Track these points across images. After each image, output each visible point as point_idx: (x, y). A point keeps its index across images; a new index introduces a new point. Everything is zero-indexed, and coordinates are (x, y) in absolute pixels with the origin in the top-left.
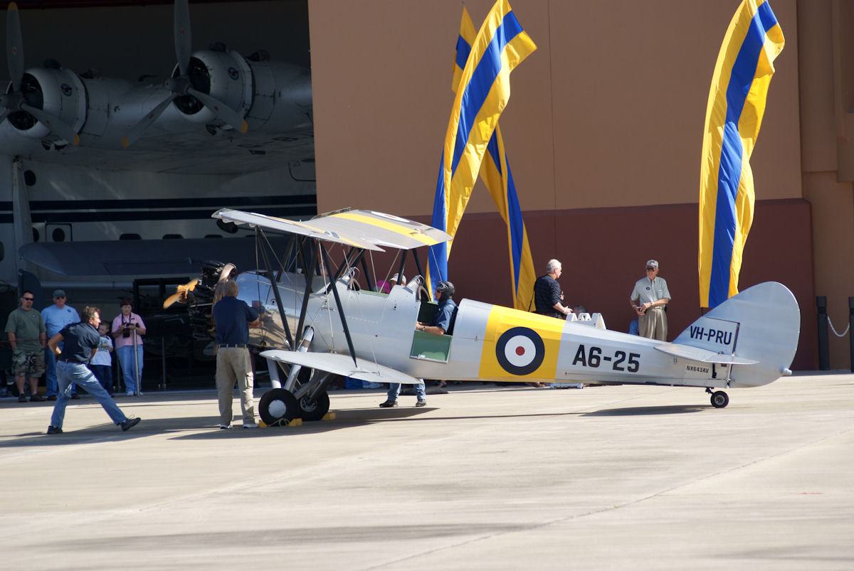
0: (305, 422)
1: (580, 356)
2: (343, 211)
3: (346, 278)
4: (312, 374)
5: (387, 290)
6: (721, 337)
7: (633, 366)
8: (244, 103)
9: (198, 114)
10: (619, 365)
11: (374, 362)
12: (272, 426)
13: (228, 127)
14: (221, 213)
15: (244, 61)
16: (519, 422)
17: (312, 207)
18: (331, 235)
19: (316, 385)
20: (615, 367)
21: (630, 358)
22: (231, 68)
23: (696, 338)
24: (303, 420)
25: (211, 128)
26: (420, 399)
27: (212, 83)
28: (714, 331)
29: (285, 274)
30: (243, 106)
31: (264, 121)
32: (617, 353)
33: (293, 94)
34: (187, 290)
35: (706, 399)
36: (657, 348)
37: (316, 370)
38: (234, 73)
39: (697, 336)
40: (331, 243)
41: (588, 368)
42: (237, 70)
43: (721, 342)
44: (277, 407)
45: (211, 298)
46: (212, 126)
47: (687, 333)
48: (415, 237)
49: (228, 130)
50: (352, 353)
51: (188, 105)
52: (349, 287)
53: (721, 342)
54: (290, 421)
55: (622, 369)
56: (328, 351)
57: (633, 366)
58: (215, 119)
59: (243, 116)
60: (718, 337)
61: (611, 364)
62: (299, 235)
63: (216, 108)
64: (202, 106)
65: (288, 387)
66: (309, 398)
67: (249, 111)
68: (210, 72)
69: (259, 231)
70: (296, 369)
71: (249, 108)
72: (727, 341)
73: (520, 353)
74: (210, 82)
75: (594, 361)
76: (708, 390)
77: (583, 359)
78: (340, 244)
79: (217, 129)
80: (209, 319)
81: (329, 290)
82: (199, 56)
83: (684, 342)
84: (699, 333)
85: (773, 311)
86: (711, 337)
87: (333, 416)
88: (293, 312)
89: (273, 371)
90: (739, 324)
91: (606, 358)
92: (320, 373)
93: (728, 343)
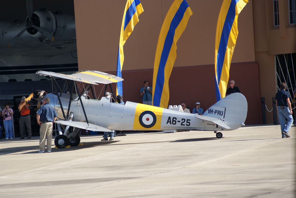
0: (72, 147)
1: (169, 121)
2: (84, 71)
3: (85, 95)
4: (74, 130)
5: (100, 99)
6: (219, 113)
7: (188, 124)
8: (53, 30)
9: (36, 34)
10: (183, 124)
11: (95, 124)
12: (60, 148)
13: (47, 39)
14: (39, 72)
15: (53, 14)
16: (147, 145)
17: (77, 68)
18: (79, 79)
19: (75, 133)
20: (182, 124)
21: (187, 121)
22: (48, 17)
23: (210, 113)
24: (71, 146)
25: (41, 39)
26: (111, 138)
27: (41, 23)
29: (63, 94)
30: (53, 31)
31: (60, 37)
32: (182, 119)
33: (70, 26)
34: (28, 100)
35: (214, 135)
36: (196, 117)
37: (75, 127)
38: (49, 19)
39: (211, 112)
40: (79, 83)
41: (172, 125)
42: (50, 18)
43: (219, 115)
44: (61, 141)
45: (37, 103)
46: (41, 39)
47: (207, 111)
48: (110, 80)
49: (47, 40)
50: (87, 121)
51: (32, 31)
52: (86, 98)
53: (219, 115)
54: (66, 146)
55: (184, 125)
56: (79, 121)
57: (188, 124)
58: (42, 36)
59: (52, 35)
60: (218, 113)
61: (180, 123)
62: (68, 80)
63: (43, 32)
64: (37, 31)
65: (65, 134)
66: (73, 138)
67: (55, 33)
68: (40, 19)
69: (53, 78)
70: (68, 128)
71: (54, 31)
72: (221, 114)
73: (148, 120)
74: (40, 22)
75: (174, 122)
76: (215, 132)
77: (170, 122)
78: (82, 82)
79: (43, 40)
81: (78, 99)
82: (36, 13)
83: (206, 115)
84: (212, 112)
85: (239, 103)
86: (216, 113)
87: (82, 144)
88: (65, 107)
89: (59, 128)
90: (226, 108)
91: (178, 121)
92: (77, 129)
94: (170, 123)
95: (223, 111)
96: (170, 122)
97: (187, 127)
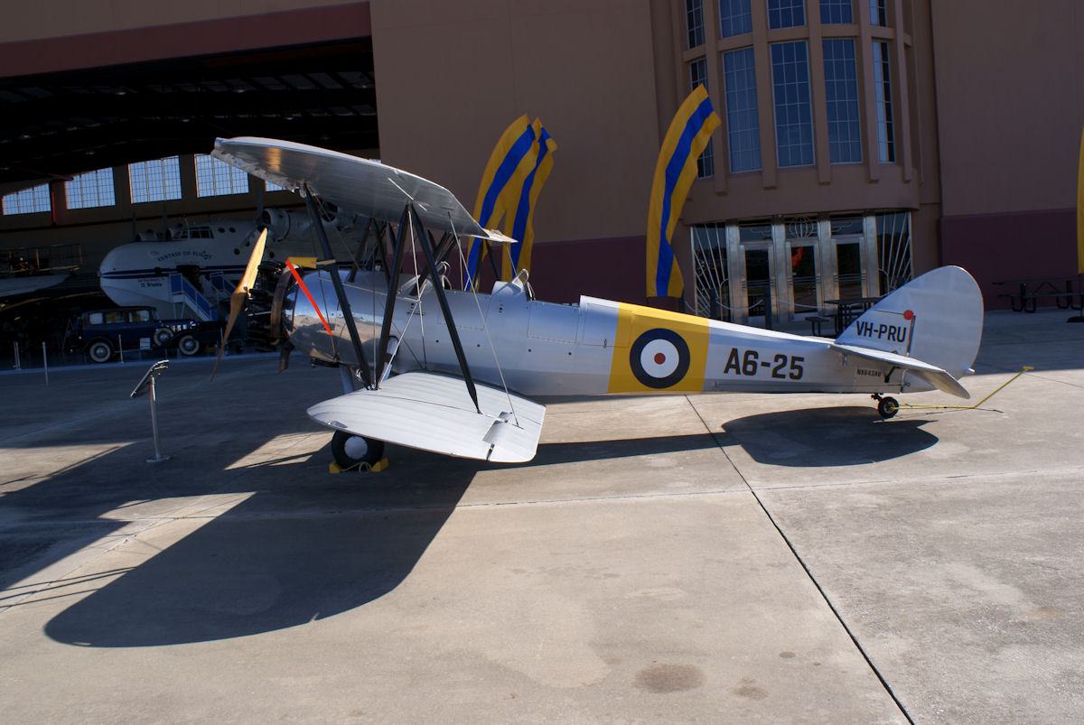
1: (733, 362)
7: (796, 372)
10: (779, 372)
20: (775, 375)
23: (865, 335)
28: (885, 326)
32: (777, 357)
41: (742, 377)
47: (852, 329)
55: (783, 376)
57: (796, 372)
60: (890, 333)
72: (901, 338)
75: (750, 368)
76: (876, 397)
77: (736, 366)
80: (268, 331)
91: (764, 364)
93: (903, 340)
94: (734, 370)
96: (736, 366)
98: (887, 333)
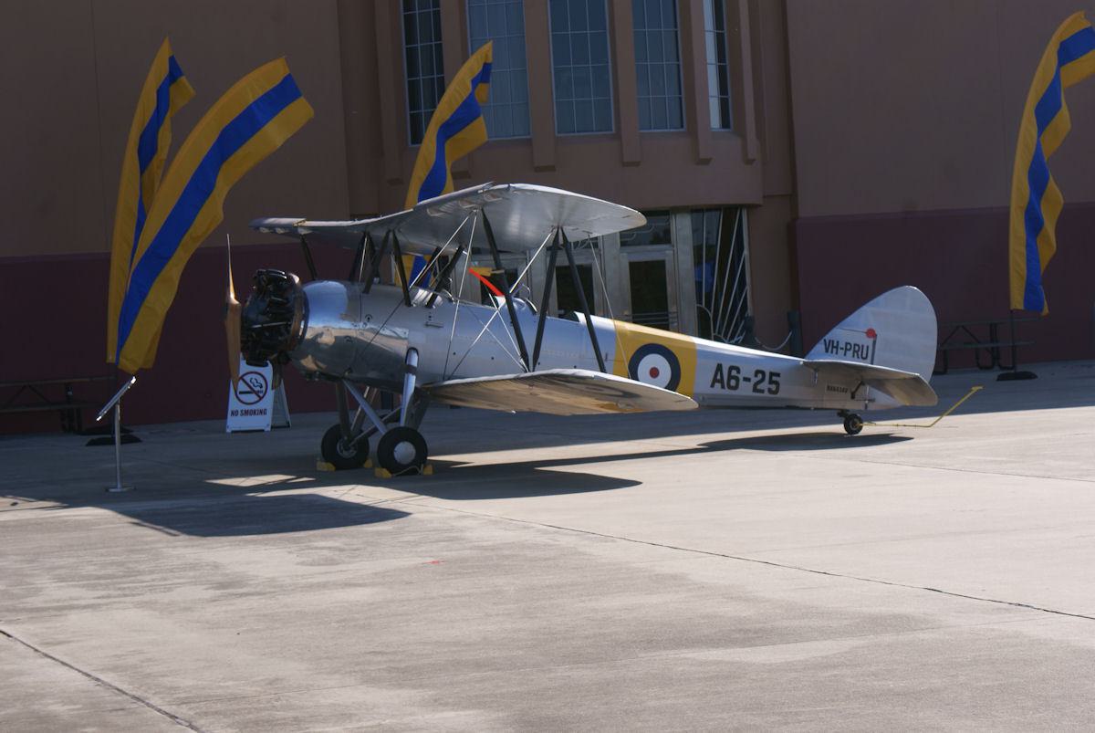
1: (719, 377)
10: (759, 387)
20: (755, 390)
21: (771, 378)
23: (832, 352)
32: (757, 372)
41: (727, 392)
47: (820, 347)
55: (762, 391)
57: (773, 387)
60: (854, 351)
72: (864, 356)
75: (733, 383)
77: (721, 381)
95: (868, 347)
97: (771, 399)
98: (852, 351)
